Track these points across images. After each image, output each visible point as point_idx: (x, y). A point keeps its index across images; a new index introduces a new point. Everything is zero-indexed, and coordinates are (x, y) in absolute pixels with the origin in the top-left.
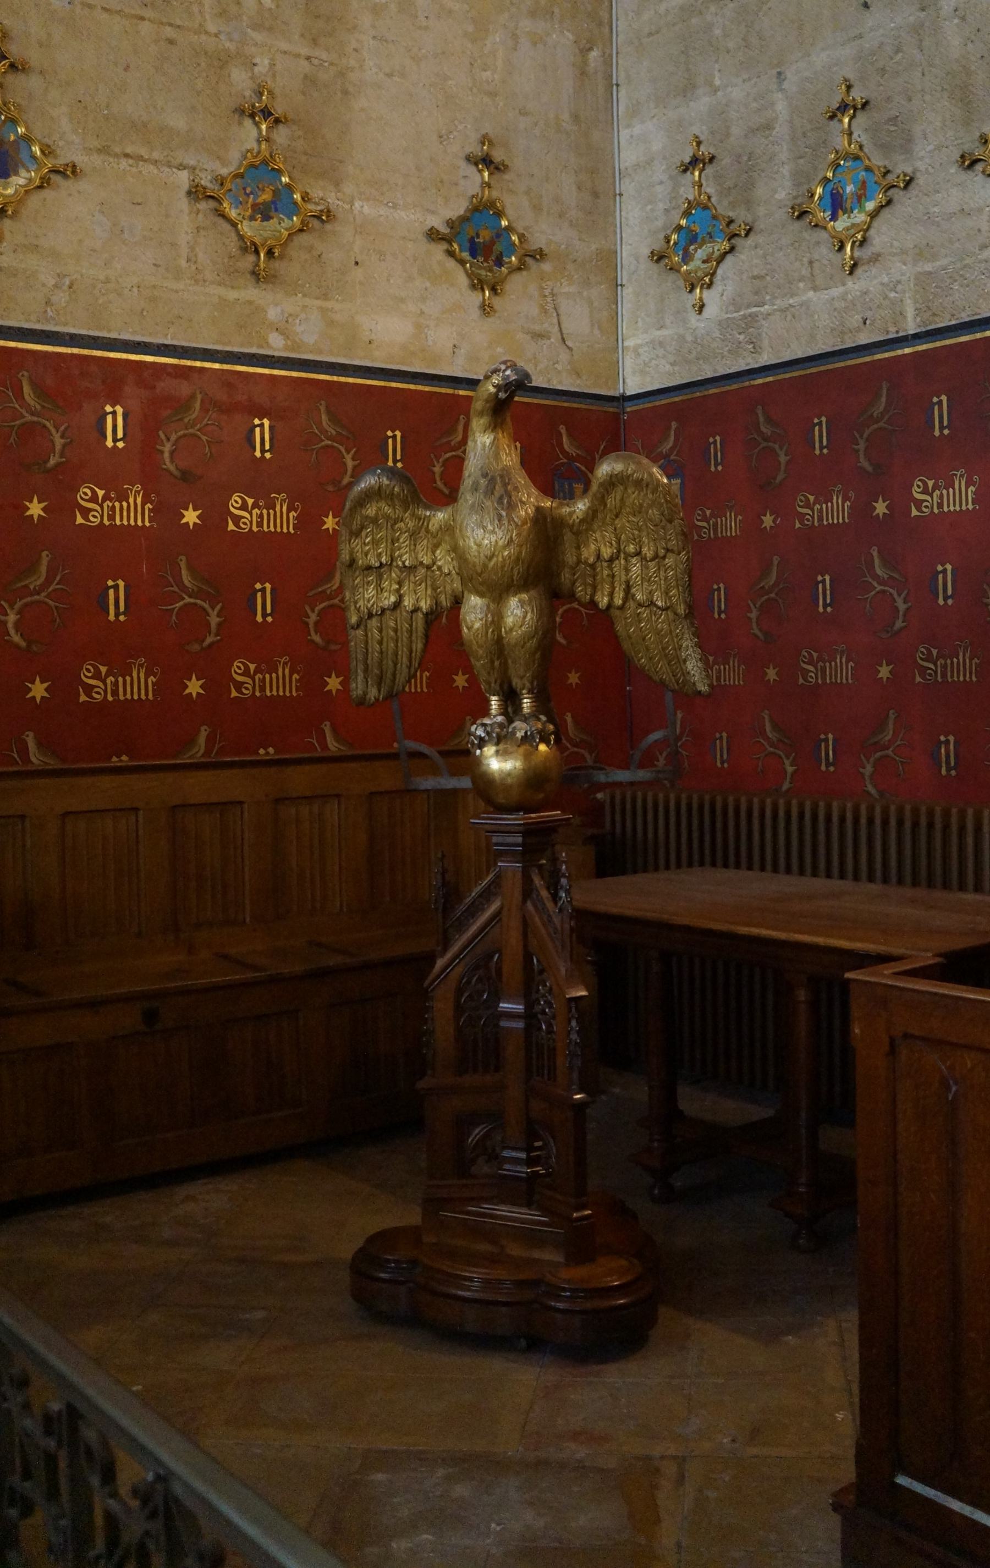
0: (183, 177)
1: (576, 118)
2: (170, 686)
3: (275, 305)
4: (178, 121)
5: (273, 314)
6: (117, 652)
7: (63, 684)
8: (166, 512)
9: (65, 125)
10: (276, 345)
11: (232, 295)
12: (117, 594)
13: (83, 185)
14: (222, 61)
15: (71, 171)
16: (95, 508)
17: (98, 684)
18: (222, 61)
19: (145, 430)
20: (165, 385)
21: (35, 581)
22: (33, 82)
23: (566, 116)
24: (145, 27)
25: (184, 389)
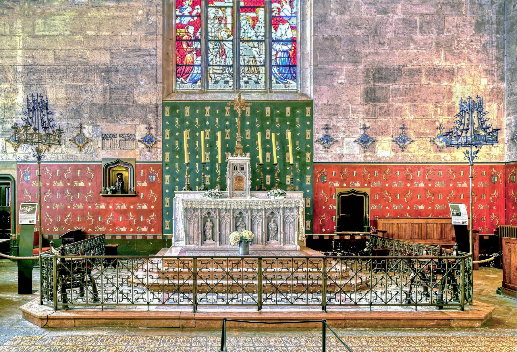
0: (429, 139)
1: (497, 117)
2: (426, 208)
3: (442, 155)
4: (428, 131)
5: (442, 156)
6: (419, 203)
7: (412, 207)
8: (426, 185)
9: (413, 135)
10: (443, 161)
11: (436, 154)
12: (419, 196)
13: (415, 143)
14: (435, 122)
15: (413, 141)
16: (416, 184)
17: (417, 207)
18: (435, 122)
19: (424, 174)
20: (426, 168)
21: (408, 194)
22: (408, 130)
23: (495, 117)
24: (424, 120)
25: (429, 168)
